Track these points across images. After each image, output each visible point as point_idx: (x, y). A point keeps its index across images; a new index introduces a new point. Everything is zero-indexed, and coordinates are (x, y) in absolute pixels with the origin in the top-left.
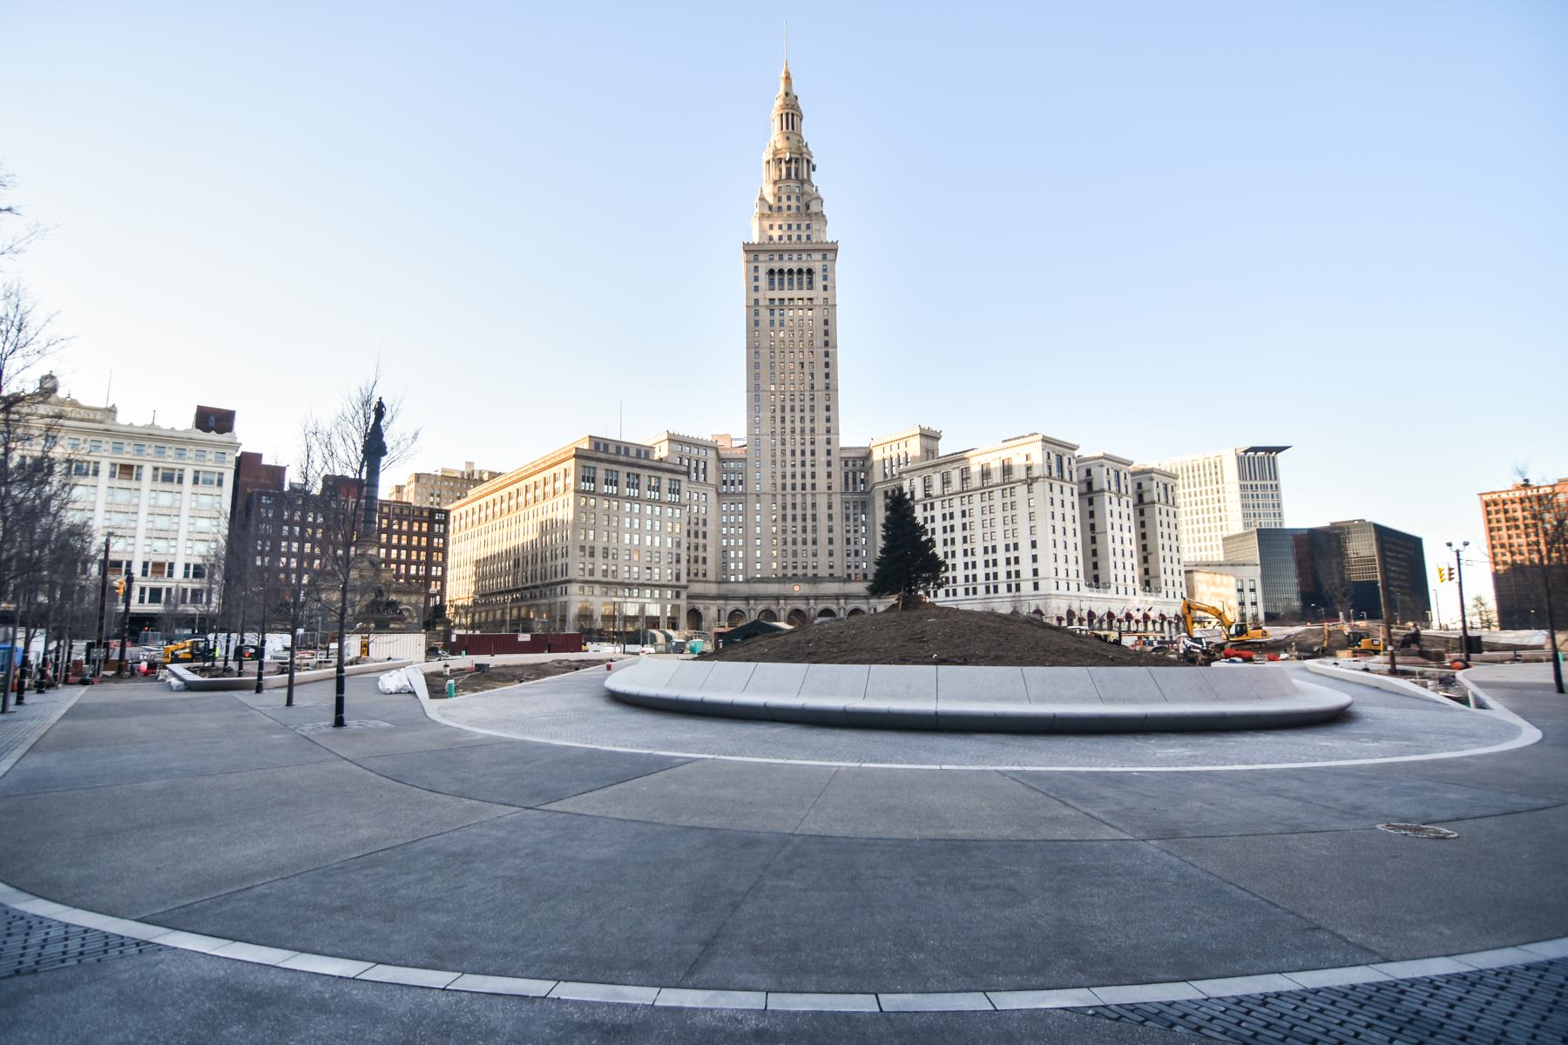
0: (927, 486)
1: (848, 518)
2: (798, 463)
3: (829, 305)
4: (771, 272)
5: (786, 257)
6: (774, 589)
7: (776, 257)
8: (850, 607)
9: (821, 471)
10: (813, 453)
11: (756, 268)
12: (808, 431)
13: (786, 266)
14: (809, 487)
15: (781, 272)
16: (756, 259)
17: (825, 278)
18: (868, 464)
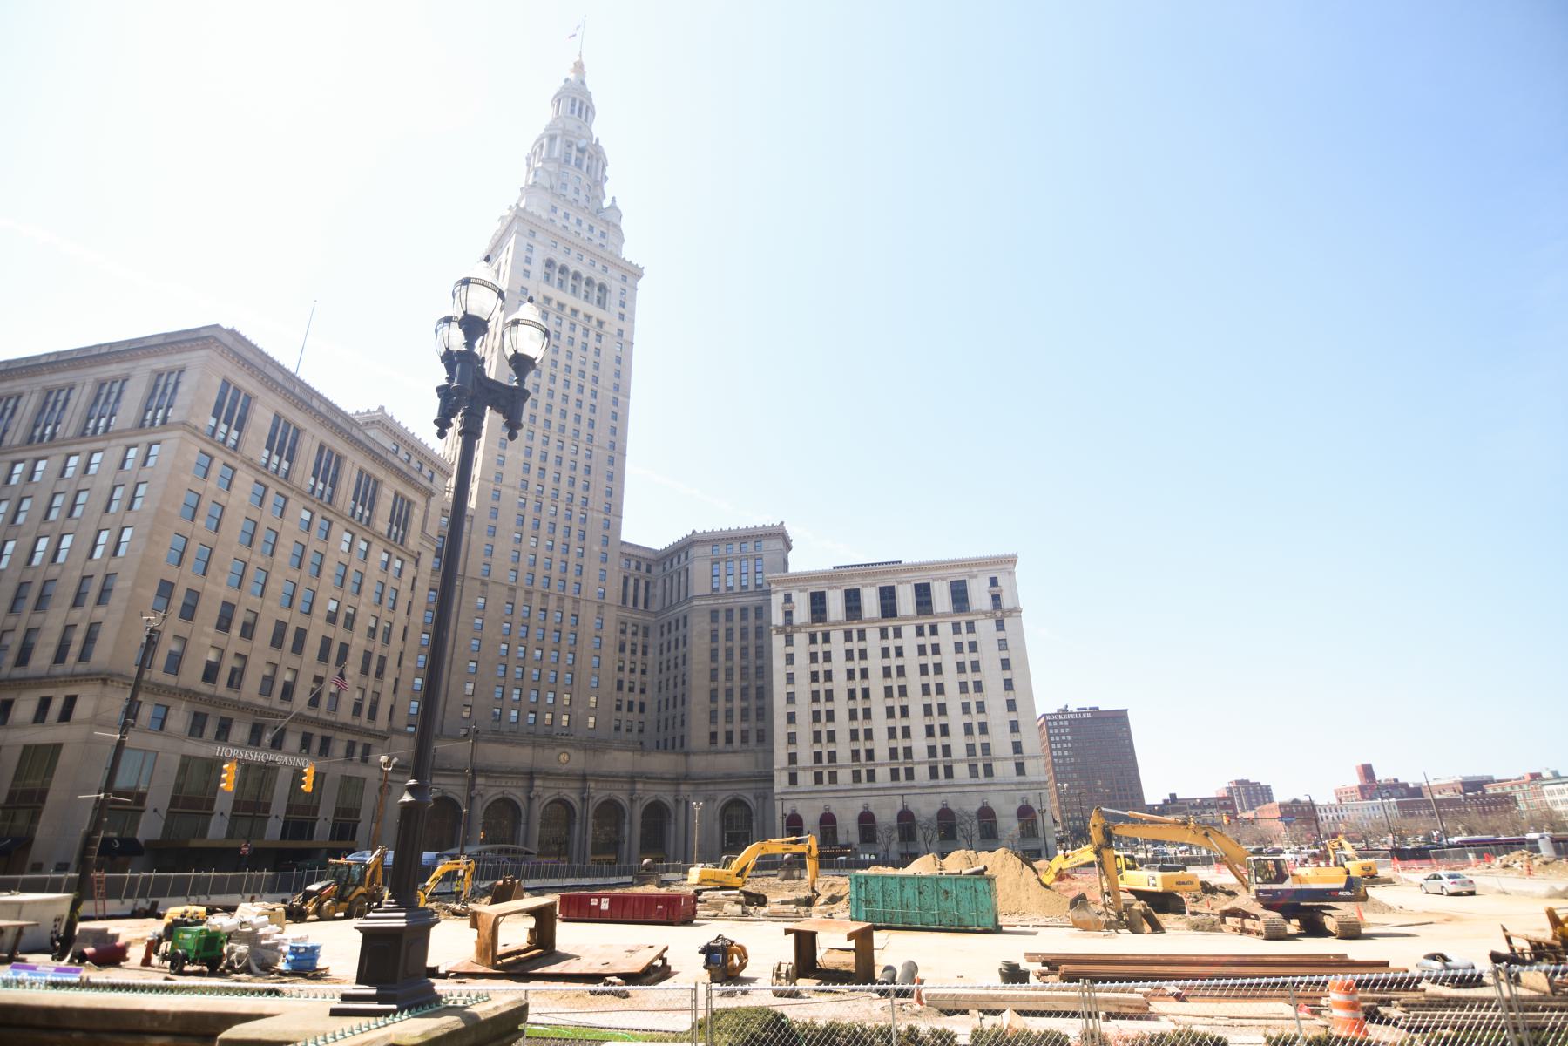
0: (818, 603)
1: (622, 649)
2: (559, 546)
3: (624, 339)
4: (550, 263)
5: (574, 253)
6: (522, 756)
7: (561, 247)
8: (649, 797)
9: (592, 567)
10: (583, 537)
11: (530, 248)
12: (578, 500)
13: (574, 266)
14: (571, 586)
15: (563, 270)
16: (532, 233)
17: (623, 304)
18: (656, 570)
